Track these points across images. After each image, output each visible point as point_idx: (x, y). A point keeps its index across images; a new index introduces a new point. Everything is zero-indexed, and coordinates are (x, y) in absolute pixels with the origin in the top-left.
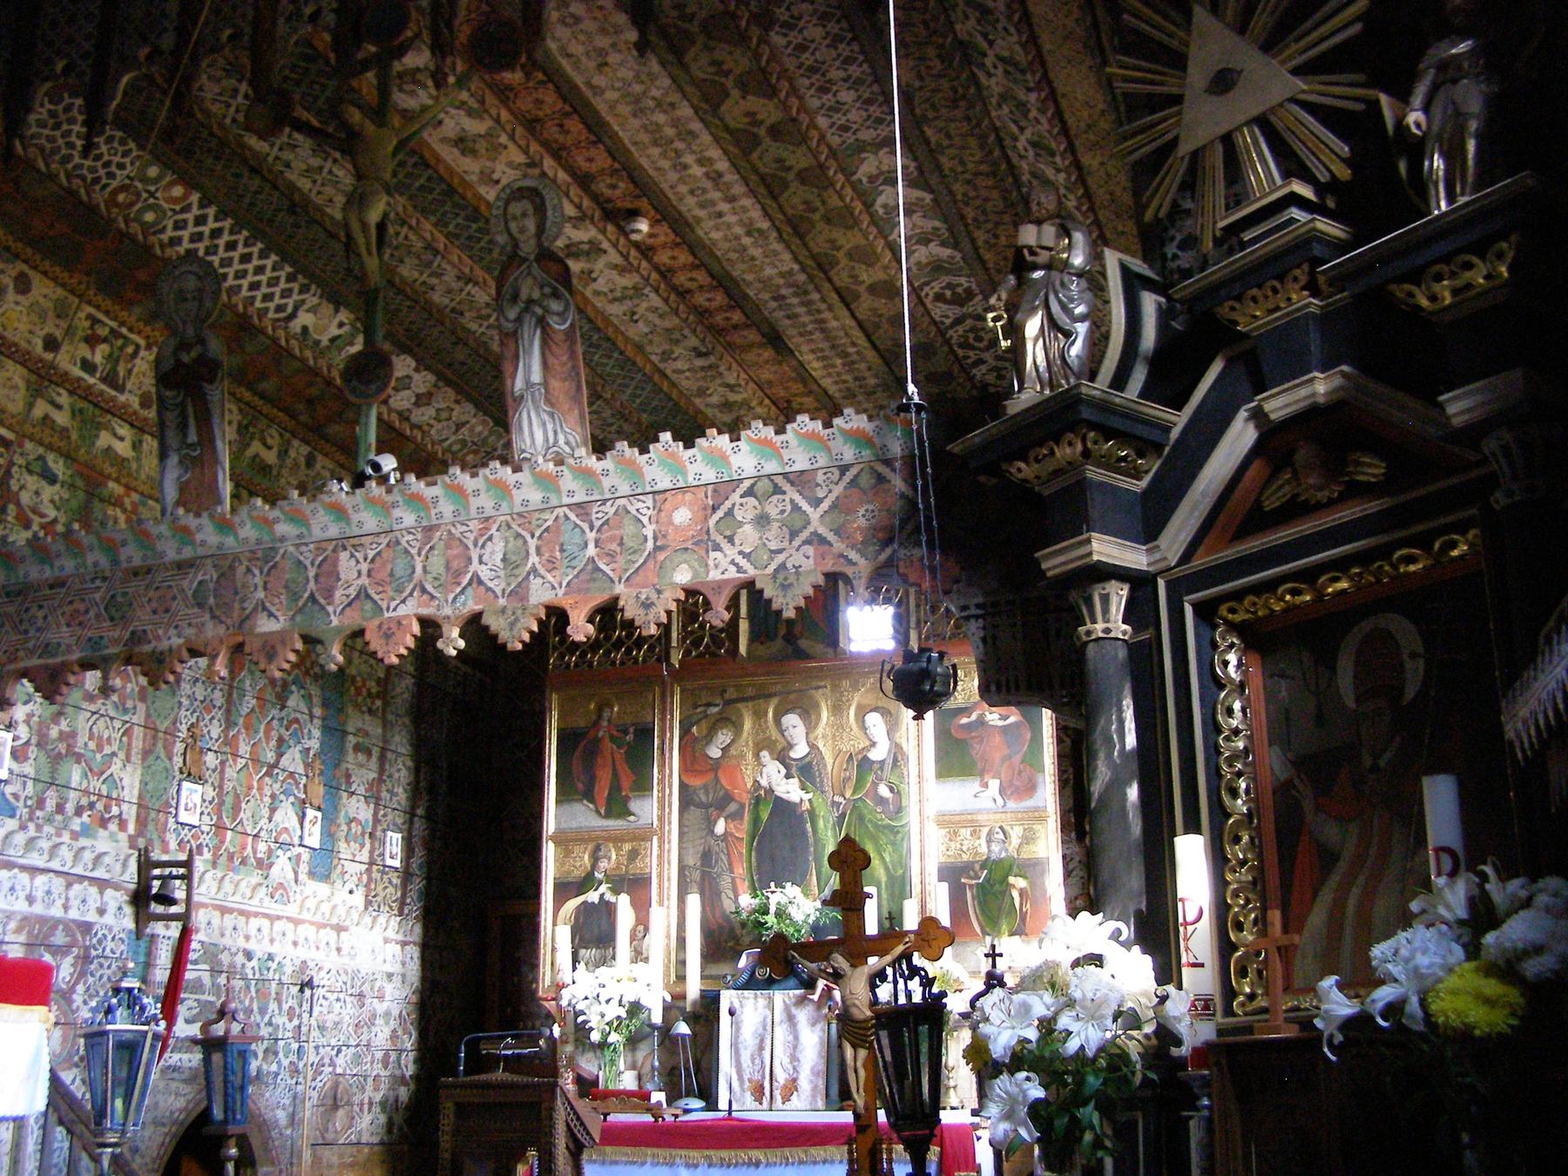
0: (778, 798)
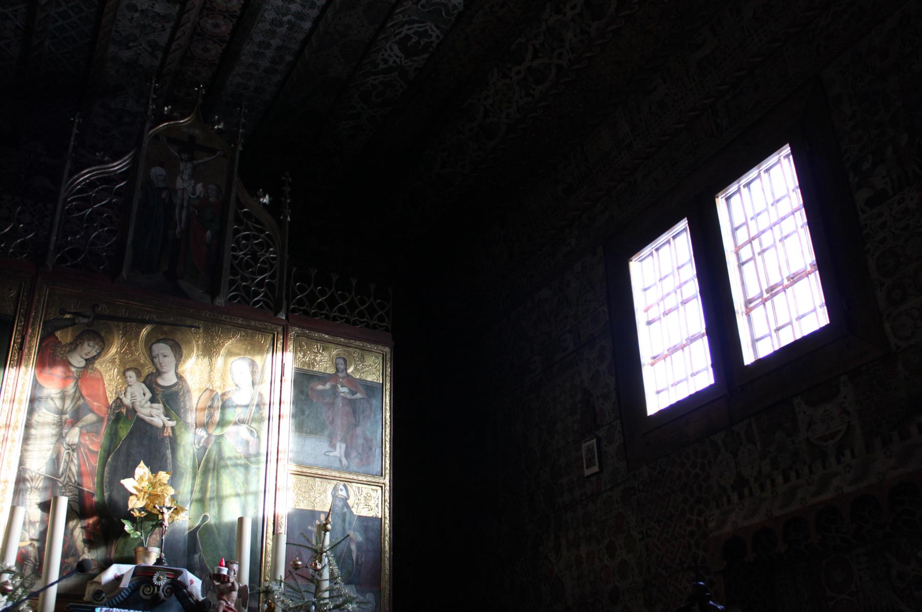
0: (141, 421)
